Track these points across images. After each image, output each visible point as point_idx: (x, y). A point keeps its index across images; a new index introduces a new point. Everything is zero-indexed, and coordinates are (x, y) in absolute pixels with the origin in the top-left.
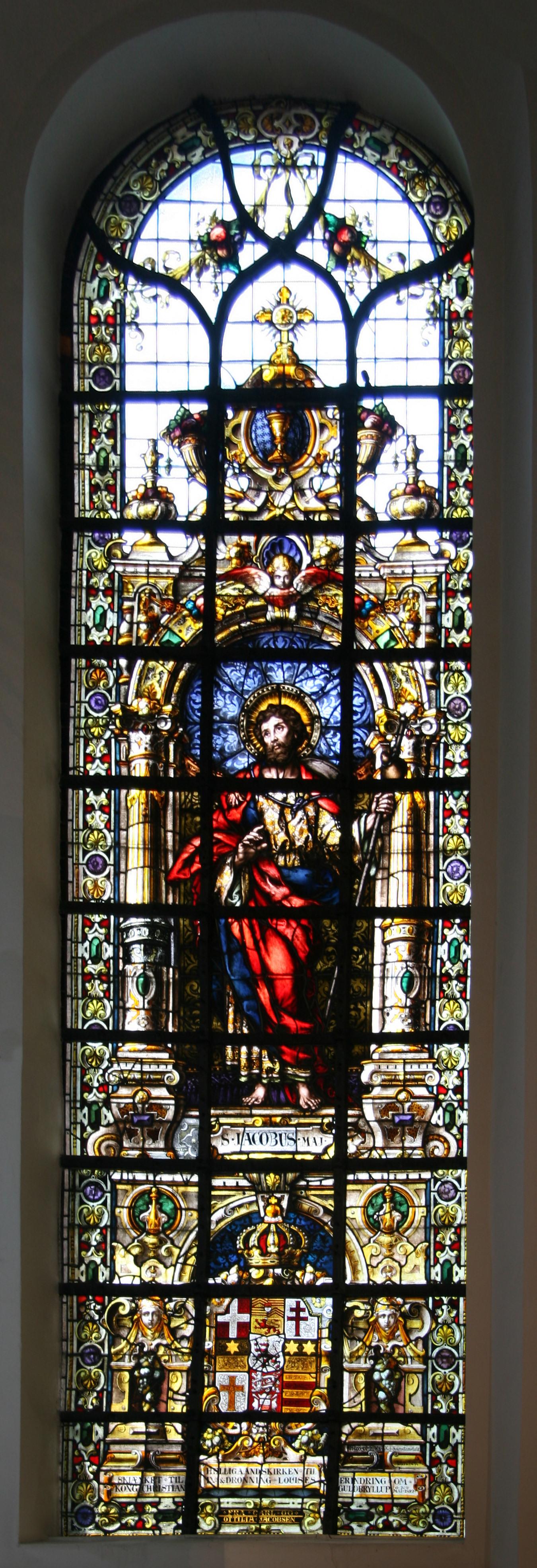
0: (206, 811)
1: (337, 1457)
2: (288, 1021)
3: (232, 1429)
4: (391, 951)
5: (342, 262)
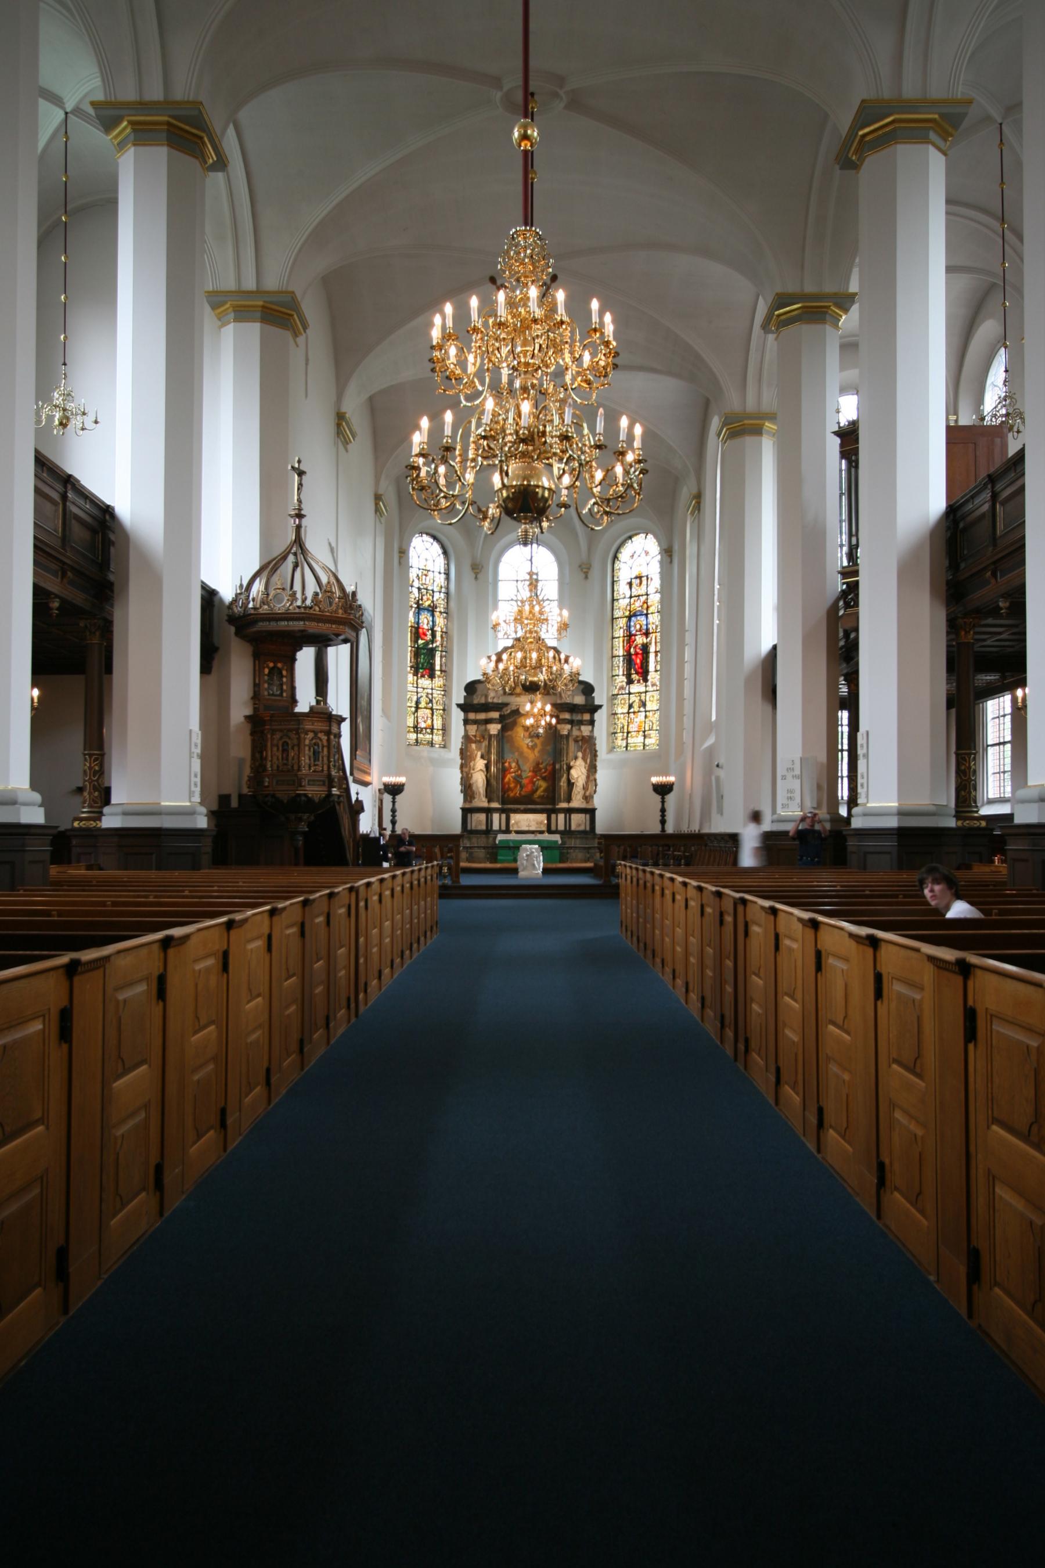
1: (645, 736)
4: (652, 657)
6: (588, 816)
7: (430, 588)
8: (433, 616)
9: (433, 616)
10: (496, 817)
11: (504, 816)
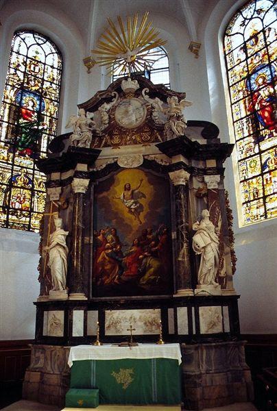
0: (252, 98)
2: (270, 123)
3: (271, 197)
5: (259, 14)
6: (226, 308)
7: (39, 76)
8: (41, 101)
9: (41, 101)
10: (78, 315)
11: (94, 315)
